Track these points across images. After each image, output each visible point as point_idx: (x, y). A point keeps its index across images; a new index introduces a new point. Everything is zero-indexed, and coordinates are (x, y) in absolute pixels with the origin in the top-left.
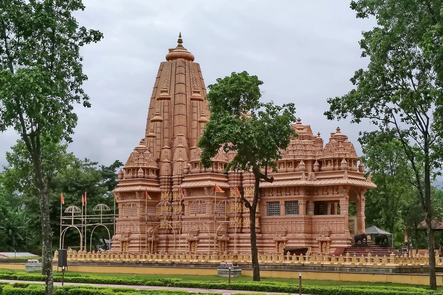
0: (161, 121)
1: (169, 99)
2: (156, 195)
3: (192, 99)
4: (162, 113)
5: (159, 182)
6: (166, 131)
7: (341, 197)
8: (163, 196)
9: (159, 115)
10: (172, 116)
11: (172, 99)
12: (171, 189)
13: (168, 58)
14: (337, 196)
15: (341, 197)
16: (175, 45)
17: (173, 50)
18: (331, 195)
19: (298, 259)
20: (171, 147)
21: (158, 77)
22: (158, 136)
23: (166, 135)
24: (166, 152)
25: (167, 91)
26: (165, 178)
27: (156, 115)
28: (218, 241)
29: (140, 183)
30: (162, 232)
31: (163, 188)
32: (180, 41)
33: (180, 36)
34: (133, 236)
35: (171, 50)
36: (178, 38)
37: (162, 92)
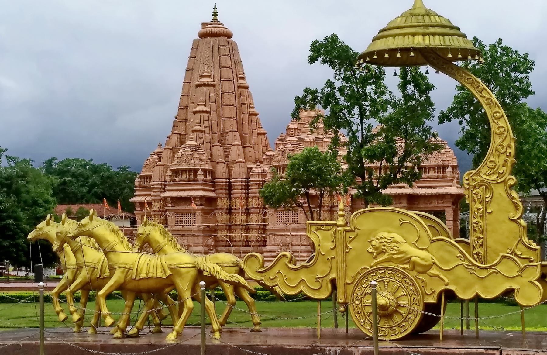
1: (214, 86)
2: (210, 201)
3: (239, 87)
4: (208, 103)
5: (214, 186)
6: (215, 125)
7: (446, 207)
8: (220, 203)
9: (204, 105)
10: (220, 107)
11: (218, 86)
13: (203, 36)
14: (443, 205)
15: (446, 207)
16: (209, 18)
17: (208, 24)
20: (222, 143)
21: (193, 57)
22: (207, 131)
23: (215, 129)
24: (218, 151)
25: (209, 76)
26: (223, 182)
27: (199, 105)
29: (202, 187)
30: (221, 244)
32: (215, 14)
33: (215, 8)
35: (204, 25)
36: (213, 10)
37: (202, 77)
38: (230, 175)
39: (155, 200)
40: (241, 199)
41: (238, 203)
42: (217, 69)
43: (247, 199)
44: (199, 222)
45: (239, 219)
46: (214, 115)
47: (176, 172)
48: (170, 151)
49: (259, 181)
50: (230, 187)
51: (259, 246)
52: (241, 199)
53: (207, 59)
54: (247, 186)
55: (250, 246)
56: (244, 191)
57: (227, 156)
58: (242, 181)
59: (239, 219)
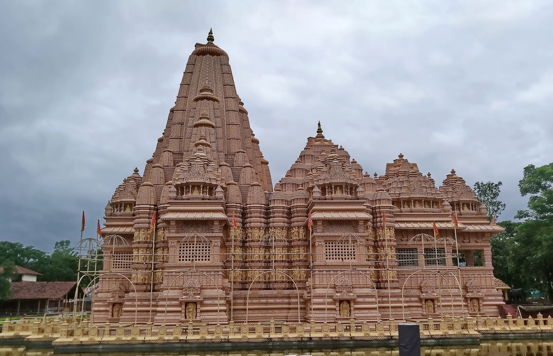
0: (213, 127)
7: (485, 246)
15: (485, 246)
16: (205, 42)
18: (473, 244)
19: (526, 323)
22: (214, 146)
24: (227, 171)
25: (212, 91)
28: (466, 299)
31: (235, 221)
34: (208, 293)
37: (201, 91)
38: (244, 200)
40: (260, 229)
41: (257, 234)
42: (220, 86)
43: (267, 229)
44: (215, 256)
45: (257, 254)
47: (181, 188)
48: (162, 170)
49: (284, 208)
50: (244, 215)
51: (284, 289)
52: (260, 229)
54: (267, 213)
55: (247, 289)
56: (263, 220)
58: (261, 208)
59: (257, 254)
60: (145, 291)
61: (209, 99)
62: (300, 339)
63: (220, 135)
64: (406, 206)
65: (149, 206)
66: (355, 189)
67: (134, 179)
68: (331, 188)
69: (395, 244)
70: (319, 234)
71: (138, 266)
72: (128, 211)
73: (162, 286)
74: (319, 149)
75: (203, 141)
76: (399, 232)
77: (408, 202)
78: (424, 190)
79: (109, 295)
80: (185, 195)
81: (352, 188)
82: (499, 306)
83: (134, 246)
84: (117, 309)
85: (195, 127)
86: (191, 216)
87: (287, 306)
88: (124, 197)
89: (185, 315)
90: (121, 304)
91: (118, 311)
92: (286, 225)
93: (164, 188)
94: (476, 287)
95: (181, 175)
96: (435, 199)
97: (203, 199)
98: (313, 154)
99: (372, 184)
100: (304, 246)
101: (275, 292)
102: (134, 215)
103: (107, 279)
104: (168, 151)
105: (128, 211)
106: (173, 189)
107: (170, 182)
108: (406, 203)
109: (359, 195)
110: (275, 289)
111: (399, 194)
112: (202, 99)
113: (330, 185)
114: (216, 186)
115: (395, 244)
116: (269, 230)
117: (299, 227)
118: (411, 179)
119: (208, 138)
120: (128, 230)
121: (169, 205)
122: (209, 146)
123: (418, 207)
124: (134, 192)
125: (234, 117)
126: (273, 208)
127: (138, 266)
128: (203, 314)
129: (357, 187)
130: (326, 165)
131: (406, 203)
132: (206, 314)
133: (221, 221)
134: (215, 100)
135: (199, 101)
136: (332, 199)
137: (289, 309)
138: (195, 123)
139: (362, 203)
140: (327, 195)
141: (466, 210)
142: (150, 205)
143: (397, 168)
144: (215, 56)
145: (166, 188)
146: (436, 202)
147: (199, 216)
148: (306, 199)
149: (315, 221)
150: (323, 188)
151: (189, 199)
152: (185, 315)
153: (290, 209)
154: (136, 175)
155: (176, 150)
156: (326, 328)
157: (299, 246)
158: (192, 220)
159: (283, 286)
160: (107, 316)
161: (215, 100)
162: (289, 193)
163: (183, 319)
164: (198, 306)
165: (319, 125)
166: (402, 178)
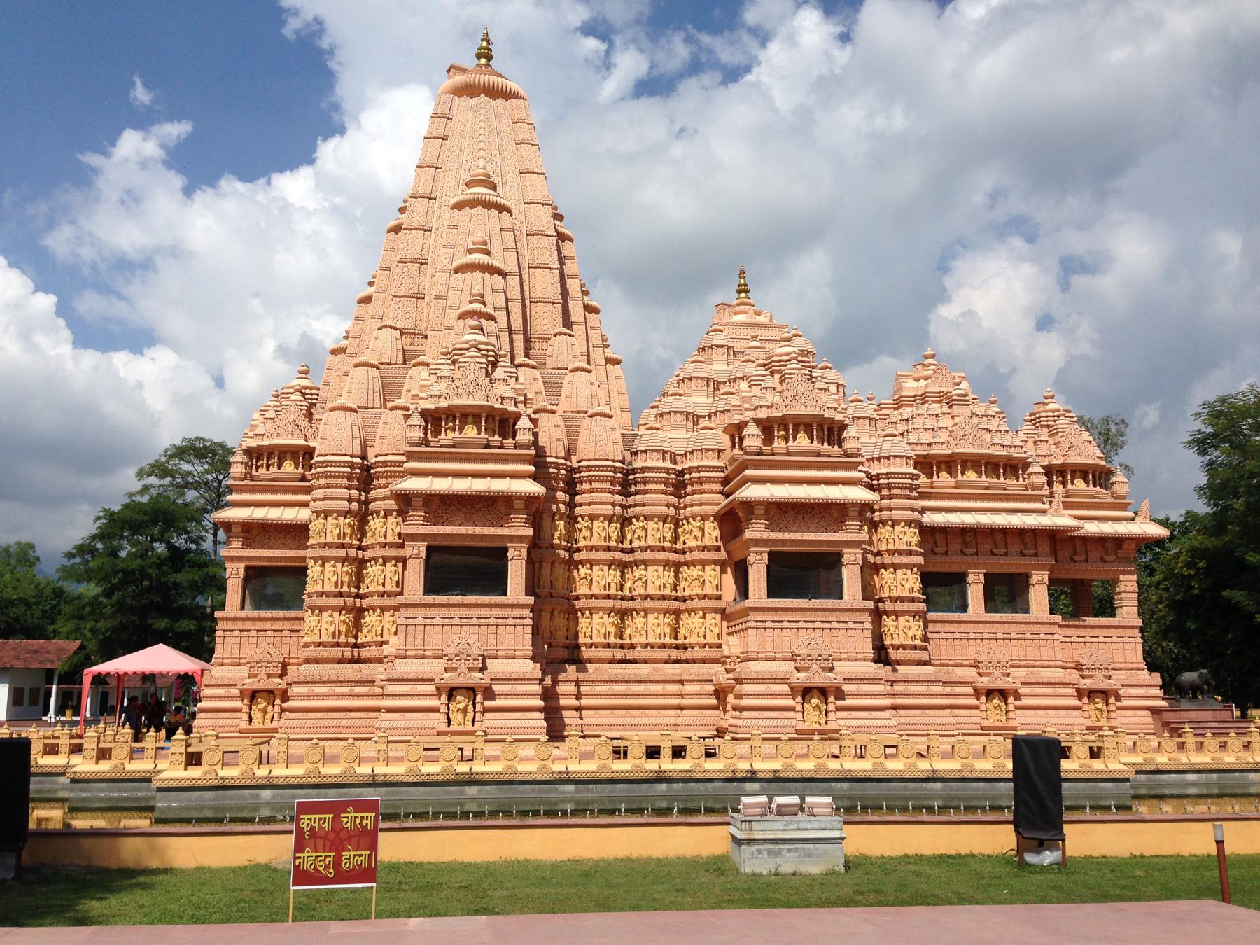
12: (571, 505)
16: (470, 62)
23: (517, 324)
25: (494, 188)
26: (558, 466)
32: (486, 54)
39: (327, 513)
43: (625, 521)
46: (513, 282)
47: (435, 419)
48: (375, 372)
49: (668, 471)
50: (571, 487)
53: (482, 145)
57: (554, 397)
60: (340, 661)
61: (488, 205)
62: (729, 775)
63: (515, 293)
64: (944, 474)
65: (348, 459)
66: (840, 435)
67: (302, 391)
68: (787, 430)
69: (921, 560)
70: (758, 536)
71: (324, 601)
72: (288, 467)
73: (387, 650)
74: (745, 333)
75: (477, 306)
76: (928, 533)
77: (950, 463)
78: (987, 436)
79: (243, 671)
80: (443, 436)
81: (832, 431)
82: (1155, 711)
83: (309, 553)
84: (261, 706)
85: (456, 272)
86: (461, 485)
87: (676, 701)
88: (279, 435)
89: (449, 719)
90: (285, 696)
91: (265, 711)
92: (672, 511)
93: (384, 416)
94: (1101, 667)
95: (425, 387)
96: (1010, 458)
97: (487, 446)
98: (730, 344)
99: (871, 419)
100: (716, 562)
101: (643, 670)
102: (303, 479)
103: (237, 633)
104: (391, 327)
105: (288, 467)
106: (417, 420)
107: (398, 402)
108: (943, 467)
109: (848, 445)
110: (645, 662)
111: (930, 445)
112: (472, 203)
113: (783, 422)
114: (518, 417)
115: (921, 560)
116: (631, 523)
117: (704, 518)
118: (956, 410)
119: (488, 299)
120: (290, 515)
121: (403, 458)
122: (490, 317)
123: (971, 476)
124: (304, 422)
125: (545, 251)
126: (643, 470)
127: (324, 601)
128: (488, 715)
129: (843, 427)
130: (772, 374)
131: (943, 467)
132: (497, 715)
133: (530, 499)
134: (502, 208)
135: (467, 210)
136: (788, 454)
137: (682, 708)
138: (458, 262)
139: (853, 467)
140: (775, 445)
141: (1080, 485)
142: (352, 456)
143: (923, 383)
144: (500, 101)
145: (388, 416)
146: (1014, 467)
147: (479, 486)
148: (720, 451)
149: (749, 505)
150: (768, 428)
151: (454, 446)
152: (449, 719)
153: (681, 473)
154: (304, 382)
155: (408, 325)
156: (785, 749)
157: (704, 563)
158: (462, 496)
159: (664, 654)
160: (235, 722)
161: (502, 208)
162: (676, 437)
163: (444, 727)
164: (479, 698)
165: (742, 274)
166: (936, 408)
